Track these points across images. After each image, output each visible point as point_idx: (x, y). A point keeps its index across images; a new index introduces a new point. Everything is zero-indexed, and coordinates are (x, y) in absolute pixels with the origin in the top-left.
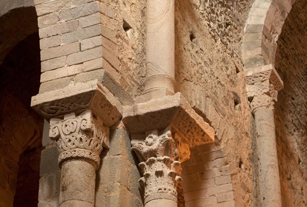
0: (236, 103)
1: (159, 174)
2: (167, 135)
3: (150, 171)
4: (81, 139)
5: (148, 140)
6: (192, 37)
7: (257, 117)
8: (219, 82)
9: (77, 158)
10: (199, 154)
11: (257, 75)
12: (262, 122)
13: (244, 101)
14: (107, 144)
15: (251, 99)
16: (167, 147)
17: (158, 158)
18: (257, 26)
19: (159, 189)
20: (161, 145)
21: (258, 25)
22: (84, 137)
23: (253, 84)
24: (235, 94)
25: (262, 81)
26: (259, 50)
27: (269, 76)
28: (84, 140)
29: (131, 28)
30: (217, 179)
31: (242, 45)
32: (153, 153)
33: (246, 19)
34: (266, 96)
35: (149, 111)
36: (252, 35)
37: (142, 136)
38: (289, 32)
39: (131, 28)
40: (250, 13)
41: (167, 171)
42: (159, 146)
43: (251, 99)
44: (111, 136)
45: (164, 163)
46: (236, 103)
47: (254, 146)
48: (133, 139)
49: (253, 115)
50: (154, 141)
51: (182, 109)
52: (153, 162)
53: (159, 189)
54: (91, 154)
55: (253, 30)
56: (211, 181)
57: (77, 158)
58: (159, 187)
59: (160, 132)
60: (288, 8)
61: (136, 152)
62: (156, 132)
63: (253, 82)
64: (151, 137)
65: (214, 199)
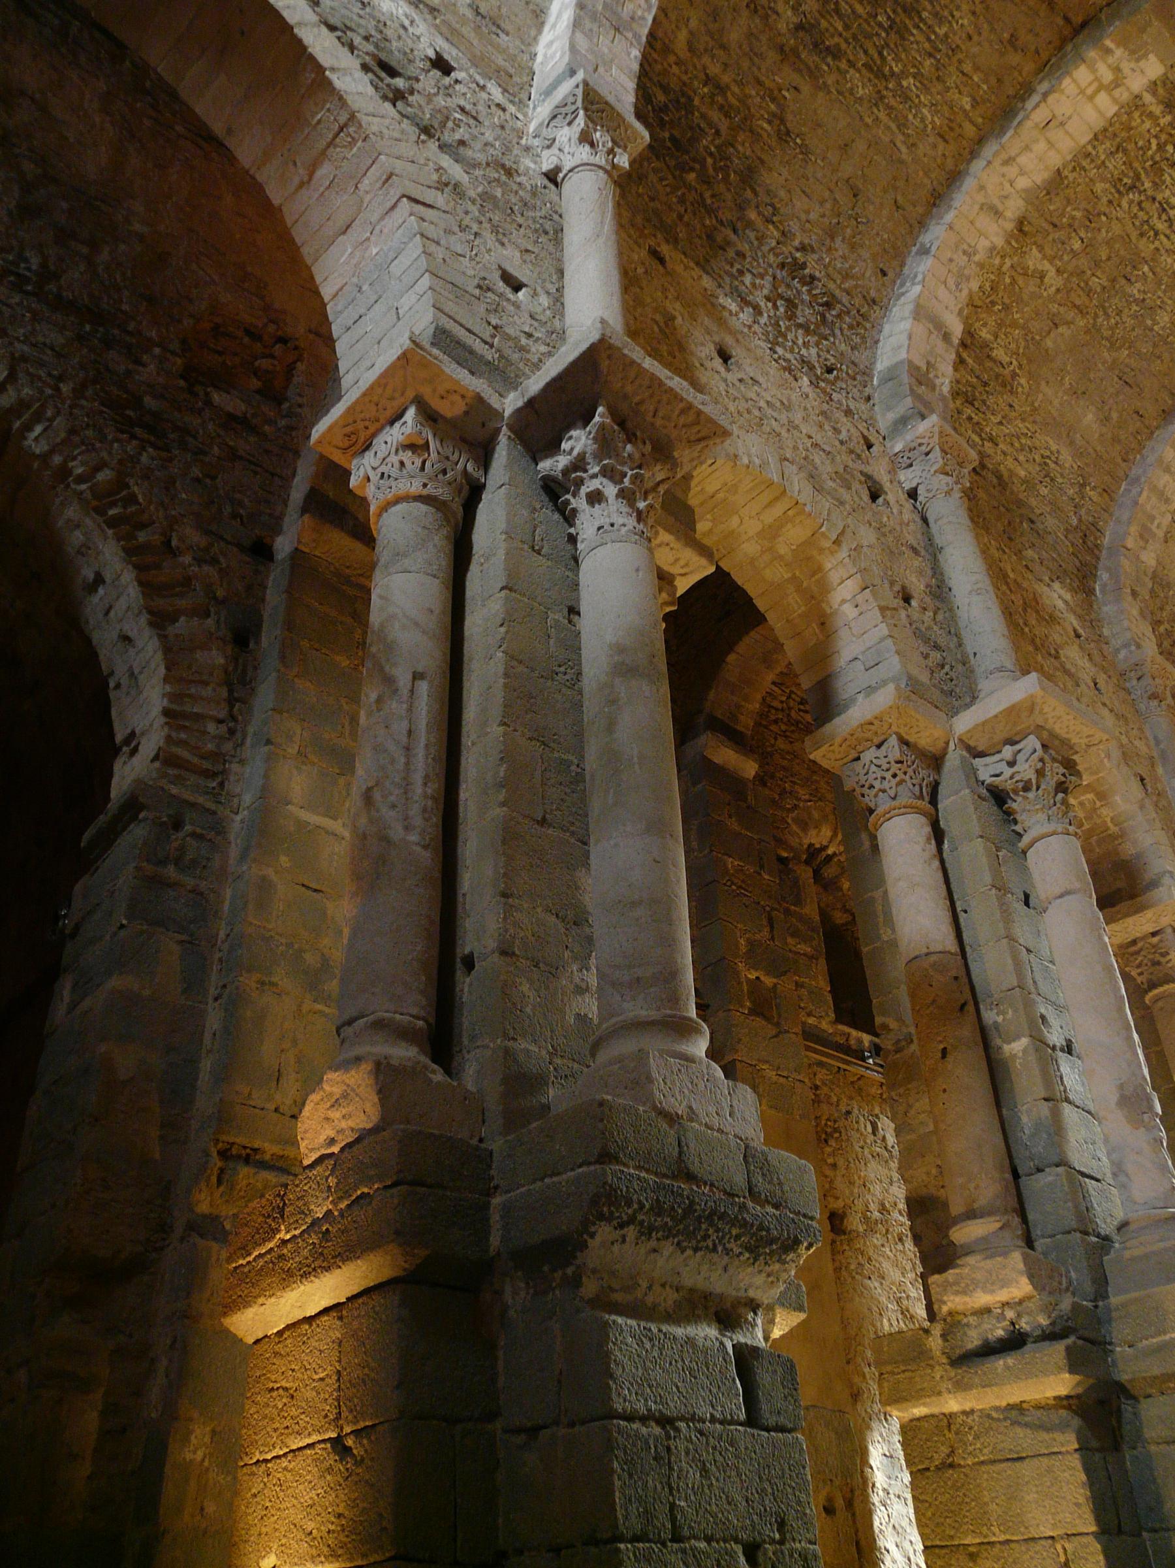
0: (874, 497)
1: (595, 498)
2: (600, 415)
3: (579, 502)
4: (402, 464)
5: (565, 446)
6: (725, 356)
7: (931, 520)
8: (816, 445)
9: (398, 500)
10: (805, 584)
11: (913, 445)
12: (939, 523)
13: (893, 496)
14: (477, 474)
15: (913, 494)
16: (605, 444)
17: (591, 472)
18: (896, 366)
19: (599, 529)
20: (590, 442)
21: (897, 364)
22: (407, 456)
23: (911, 465)
24: (868, 477)
25: (927, 454)
26: (909, 401)
27: (936, 439)
28: (408, 463)
29: (526, 286)
30: (853, 624)
31: (876, 408)
32: (579, 464)
33: (874, 363)
34: (942, 476)
35: (548, 379)
36: (890, 383)
37: (553, 447)
38: (981, 389)
39: (526, 286)
40: (879, 352)
41: (611, 490)
42: (586, 446)
43: (913, 494)
44: (485, 462)
45: (604, 476)
46: (874, 497)
47: (937, 571)
48: (541, 459)
49: (925, 520)
50: (579, 441)
51: (611, 347)
52: (580, 482)
53: (599, 529)
54: (425, 485)
55: (890, 376)
56: (844, 633)
57: (398, 500)
58: (597, 524)
59: (587, 419)
60: (957, 329)
61: (552, 484)
62: (580, 424)
63: (909, 462)
64: (571, 438)
65: (859, 666)
